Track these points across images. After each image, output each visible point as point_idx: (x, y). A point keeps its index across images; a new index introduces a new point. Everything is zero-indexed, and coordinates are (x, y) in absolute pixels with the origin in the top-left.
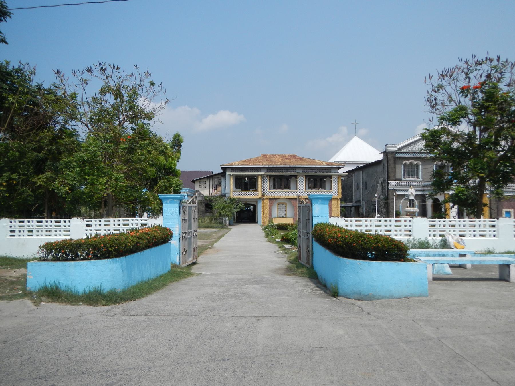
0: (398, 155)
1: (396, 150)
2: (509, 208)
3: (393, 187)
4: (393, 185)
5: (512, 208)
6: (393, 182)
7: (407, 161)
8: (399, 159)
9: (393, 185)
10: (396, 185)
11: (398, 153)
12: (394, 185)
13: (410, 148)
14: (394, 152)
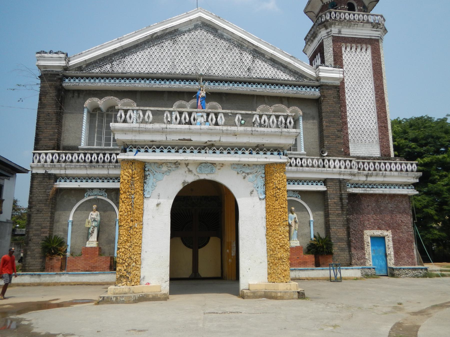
0: (68, 84)
1: (66, 68)
2: (380, 228)
3: (43, 166)
4: (46, 162)
5: (388, 227)
6: (46, 154)
7: (96, 100)
8: (76, 94)
9: (46, 162)
10: (55, 161)
11: (72, 77)
12: (49, 160)
13: (108, 67)
14: (58, 75)
